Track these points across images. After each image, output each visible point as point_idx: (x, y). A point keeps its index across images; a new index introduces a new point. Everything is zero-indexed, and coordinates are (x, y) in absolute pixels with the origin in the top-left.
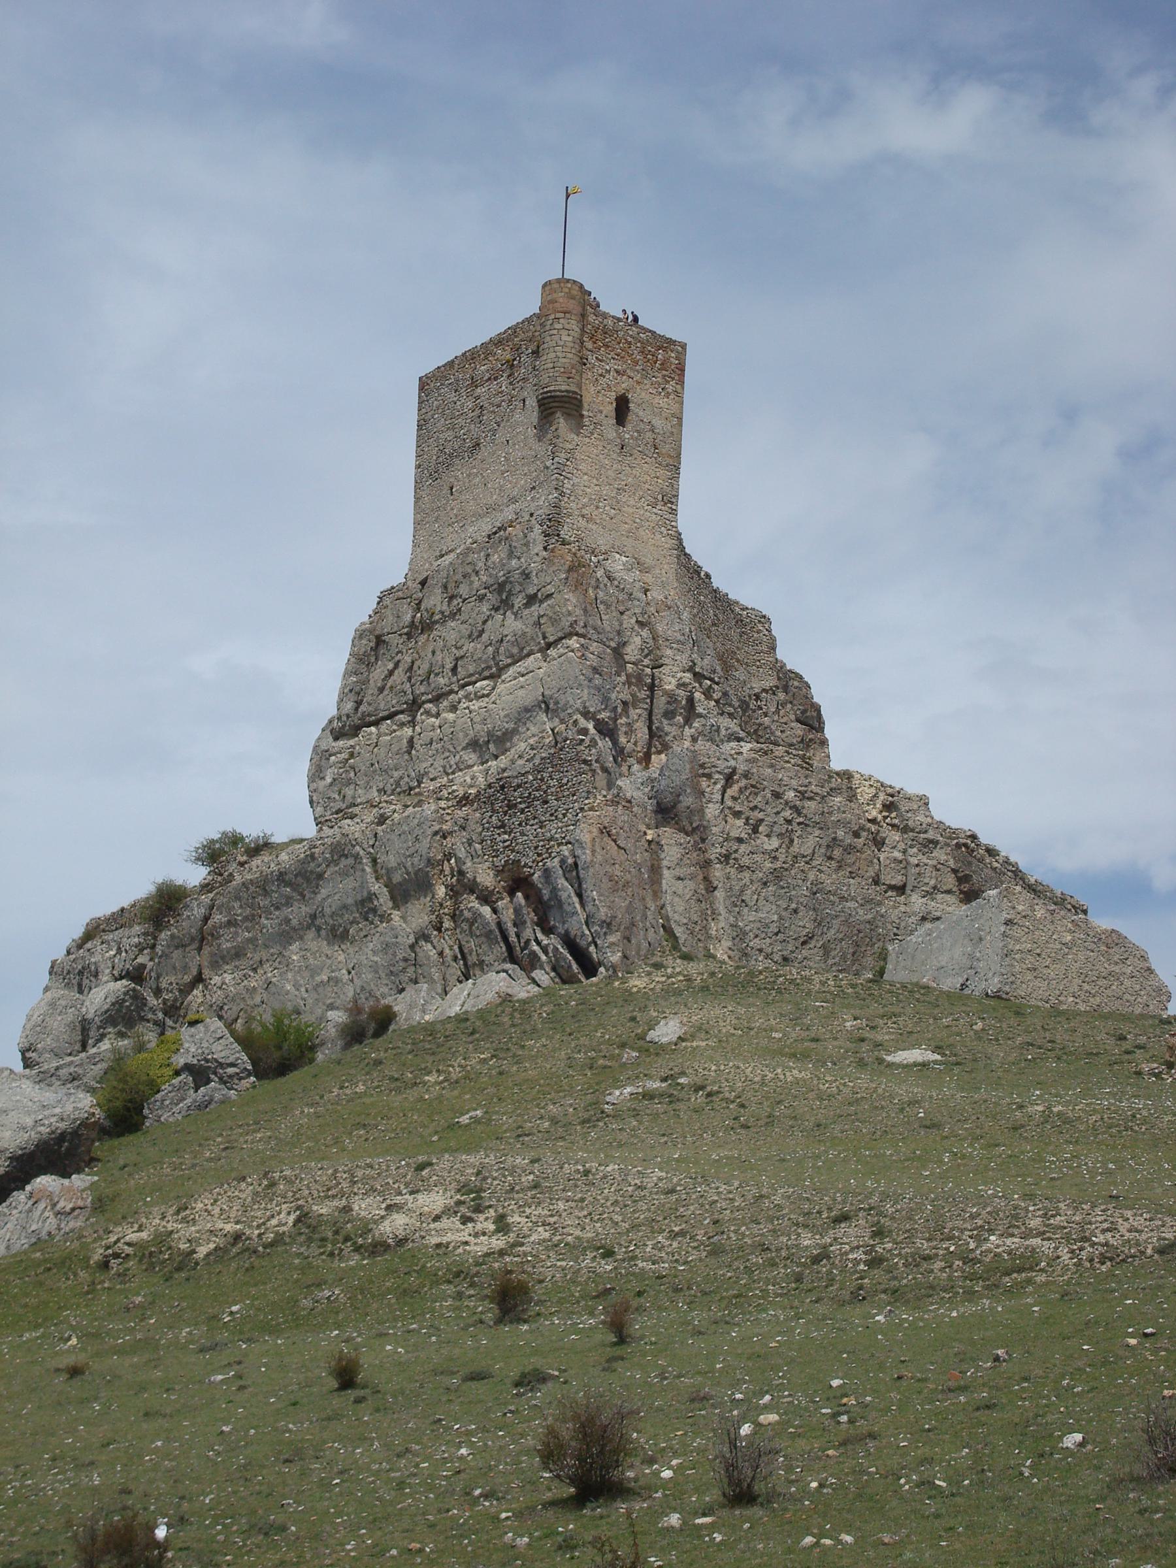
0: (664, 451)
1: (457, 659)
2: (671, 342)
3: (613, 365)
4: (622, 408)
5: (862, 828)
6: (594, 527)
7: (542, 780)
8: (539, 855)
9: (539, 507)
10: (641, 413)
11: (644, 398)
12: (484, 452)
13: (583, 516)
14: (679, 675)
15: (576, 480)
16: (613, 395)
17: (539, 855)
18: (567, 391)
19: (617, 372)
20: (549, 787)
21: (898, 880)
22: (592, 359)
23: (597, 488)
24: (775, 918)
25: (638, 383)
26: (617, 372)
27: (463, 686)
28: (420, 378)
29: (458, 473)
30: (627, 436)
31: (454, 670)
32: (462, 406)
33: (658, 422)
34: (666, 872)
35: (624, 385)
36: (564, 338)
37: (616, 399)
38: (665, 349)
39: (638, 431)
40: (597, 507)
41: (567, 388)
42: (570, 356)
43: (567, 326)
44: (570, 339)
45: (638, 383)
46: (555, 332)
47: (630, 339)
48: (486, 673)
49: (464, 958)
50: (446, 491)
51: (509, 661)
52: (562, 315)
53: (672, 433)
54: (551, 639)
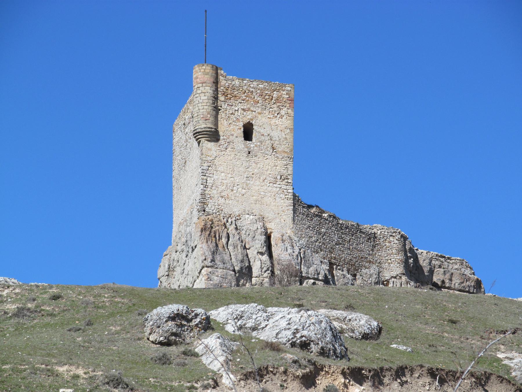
0: (280, 150)
3: (240, 106)
6: (230, 202)
10: (262, 131)
13: (222, 197)
16: (241, 124)
18: (205, 128)
23: (232, 179)
25: (259, 113)
26: (244, 110)
30: (252, 146)
33: (275, 134)
35: (248, 117)
36: (202, 98)
37: (244, 126)
39: (261, 142)
40: (232, 190)
41: (205, 126)
43: (204, 91)
44: (206, 98)
45: (259, 113)
46: (198, 95)
47: (251, 90)
52: (201, 85)
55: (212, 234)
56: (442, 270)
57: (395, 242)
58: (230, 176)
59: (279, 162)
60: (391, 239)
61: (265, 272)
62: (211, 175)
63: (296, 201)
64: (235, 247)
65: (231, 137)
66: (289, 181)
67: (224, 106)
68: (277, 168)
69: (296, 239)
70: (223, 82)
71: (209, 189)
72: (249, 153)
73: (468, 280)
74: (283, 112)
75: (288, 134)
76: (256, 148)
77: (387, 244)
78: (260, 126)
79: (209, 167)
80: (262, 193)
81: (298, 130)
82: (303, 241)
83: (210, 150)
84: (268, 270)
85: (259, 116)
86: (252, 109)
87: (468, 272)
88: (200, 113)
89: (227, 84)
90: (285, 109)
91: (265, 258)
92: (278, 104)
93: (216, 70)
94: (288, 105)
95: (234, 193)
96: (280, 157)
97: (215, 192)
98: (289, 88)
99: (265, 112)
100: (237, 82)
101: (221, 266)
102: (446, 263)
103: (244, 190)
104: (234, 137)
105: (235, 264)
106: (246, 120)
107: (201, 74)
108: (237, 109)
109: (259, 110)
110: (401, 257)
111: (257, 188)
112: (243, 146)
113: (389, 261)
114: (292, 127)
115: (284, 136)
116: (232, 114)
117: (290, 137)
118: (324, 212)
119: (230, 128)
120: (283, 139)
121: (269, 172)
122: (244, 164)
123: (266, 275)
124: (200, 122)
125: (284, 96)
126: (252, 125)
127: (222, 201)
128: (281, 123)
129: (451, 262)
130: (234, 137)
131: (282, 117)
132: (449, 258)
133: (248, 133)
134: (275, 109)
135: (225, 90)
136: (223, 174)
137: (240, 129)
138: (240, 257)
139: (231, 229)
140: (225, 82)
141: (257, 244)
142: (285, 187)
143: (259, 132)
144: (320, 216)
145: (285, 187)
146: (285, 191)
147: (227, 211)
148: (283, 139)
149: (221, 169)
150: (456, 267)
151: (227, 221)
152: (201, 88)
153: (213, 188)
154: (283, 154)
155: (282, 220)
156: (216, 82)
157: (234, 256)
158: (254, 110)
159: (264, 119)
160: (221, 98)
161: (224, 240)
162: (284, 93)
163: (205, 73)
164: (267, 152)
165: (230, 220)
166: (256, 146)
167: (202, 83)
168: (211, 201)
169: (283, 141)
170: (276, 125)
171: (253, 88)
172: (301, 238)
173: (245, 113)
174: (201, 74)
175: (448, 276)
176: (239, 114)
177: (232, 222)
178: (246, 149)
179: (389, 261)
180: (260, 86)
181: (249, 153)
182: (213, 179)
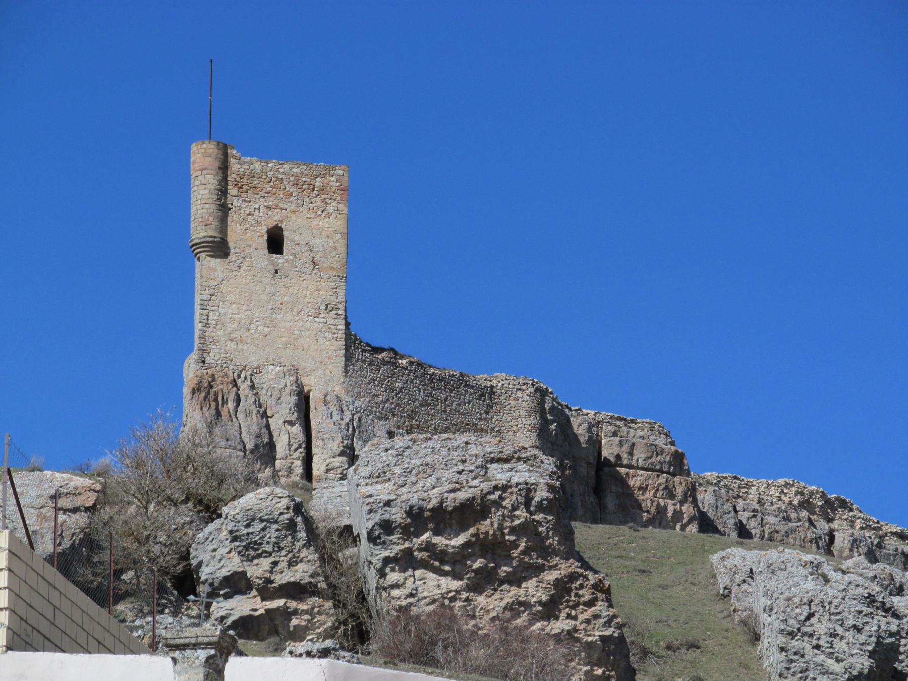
3: (263, 202)
6: (245, 347)
10: (297, 238)
13: (232, 340)
14: (328, 461)
15: (222, 311)
16: (264, 229)
23: (249, 313)
25: (293, 212)
26: (269, 208)
30: (281, 261)
33: (318, 242)
35: (274, 218)
36: (202, 192)
39: (294, 254)
40: (248, 330)
42: (207, 206)
43: (204, 181)
44: (207, 191)
45: (293, 212)
47: (280, 176)
53: (335, 248)
55: (212, 396)
56: (617, 439)
57: (524, 401)
58: (244, 308)
59: (323, 284)
60: (519, 394)
61: (296, 450)
63: (351, 342)
64: (248, 414)
65: (247, 249)
66: (340, 312)
67: (237, 203)
68: (321, 293)
69: (349, 399)
70: (235, 167)
71: (211, 329)
72: (276, 272)
73: (662, 451)
74: (330, 209)
75: (338, 241)
76: (286, 264)
77: (513, 403)
78: (294, 231)
79: (211, 295)
80: (296, 332)
81: (352, 235)
82: (362, 403)
83: (214, 270)
84: (300, 447)
85: (293, 216)
86: (281, 205)
87: (661, 441)
88: (198, 216)
89: (242, 170)
90: (334, 203)
91: (297, 429)
92: (323, 197)
93: (224, 150)
94: (339, 198)
95: (251, 335)
96: (326, 277)
97: (221, 333)
98: (341, 172)
100: (258, 166)
101: (223, 443)
102: (625, 429)
103: (266, 329)
104: (252, 249)
105: (246, 440)
106: (272, 223)
107: (202, 155)
108: (257, 206)
109: (293, 207)
110: (534, 421)
111: (288, 324)
112: (266, 262)
113: (515, 428)
114: (345, 231)
115: (332, 244)
116: (249, 214)
117: (342, 246)
118: (402, 357)
119: (247, 235)
120: (329, 249)
121: (307, 300)
122: (268, 289)
123: (297, 454)
124: (198, 228)
125: (331, 184)
126: (281, 229)
127: (233, 345)
128: (327, 225)
129: (636, 427)
130: (252, 249)
131: (329, 216)
132: (632, 421)
133: (275, 242)
134: (319, 204)
135: (238, 179)
136: (234, 306)
137: (262, 236)
138: (255, 429)
139: (244, 387)
140: (239, 166)
141: (282, 411)
142: (332, 322)
143: (292, 240)
144: (395, 364)
145: (332, 322)
146: (332, 327)
147: (239, 361)
148: (329, 249)
150: (641, 434)
151: (239, 377)
152: (199, 178)
153: (218, 327)
154: (330, 272)
155: (327, 371)
156: (224, 167)
157: (248, 427)
158: (285, 206)
159: (300, 220)
160: (233, 191)
161: (231, 405)
162: (332, 179)
163: (206, 155)
164: (305, 270)
165: (243, 375)
166: (287, 261)
167: (202, 170)
168: (214, 347)
169: (330, 252)
170: (320, 229)
171: (283, 173)
172: (358, 396)
173: (270, 212)
174: (202, 155)
175: (626, 448)
176: (261, 214)
177: (246, 378)
178: (271, 267)
179: (515, 428)
180: (295, 170)
181: (276, 272)
182: (217, 314)
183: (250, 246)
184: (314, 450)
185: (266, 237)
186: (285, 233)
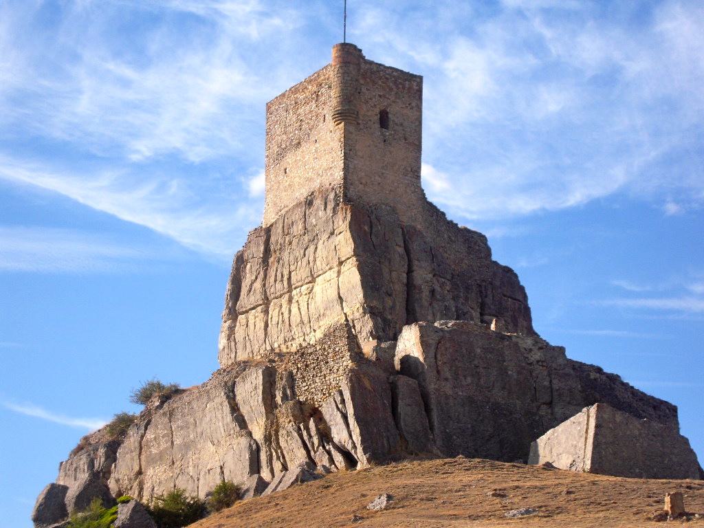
1: (290, 273)
2: (415, 76)
4: (384, 120)
5: (523, 368)
7: (324, 349)
8: (324, 394)
9: (334, 180)
11: (397, 111)
12: (304, 146)
13: (361, 183)
15: (356, 162)
16: (377, 111)
17: (324, 394)
19: (380, 96)
20: (328, 353)
21: (547, 398)
22: (364, 90)
24: (469, 426)
26: (380, 96)
27: (295, 288)
28: (267, 104)
29: (290, 159)
30: (387, 134)
31: (289, 279)
32: (290, 120)
33: (406, 124)
34: (400, 401)
38: (410, 81)
42: (349, 88)
47: (387, 76)
48: (306, 281)
49: (284, 457)
50: (283, 171)
51: (321, 272)
54: (343, 259)
62: (352, 160)
65: (369, 122)
72: (385, 141)
77: (477, 248)
85: (393, 104)
99: (398, 100)
127: (361, 186)
149: (360, 154)
166: (391, 134)
171: (388, 74)
181: (385, 141)
183: (370, 120)
184: (415, 268)
185: (379, 115)
186: (390, 116)
